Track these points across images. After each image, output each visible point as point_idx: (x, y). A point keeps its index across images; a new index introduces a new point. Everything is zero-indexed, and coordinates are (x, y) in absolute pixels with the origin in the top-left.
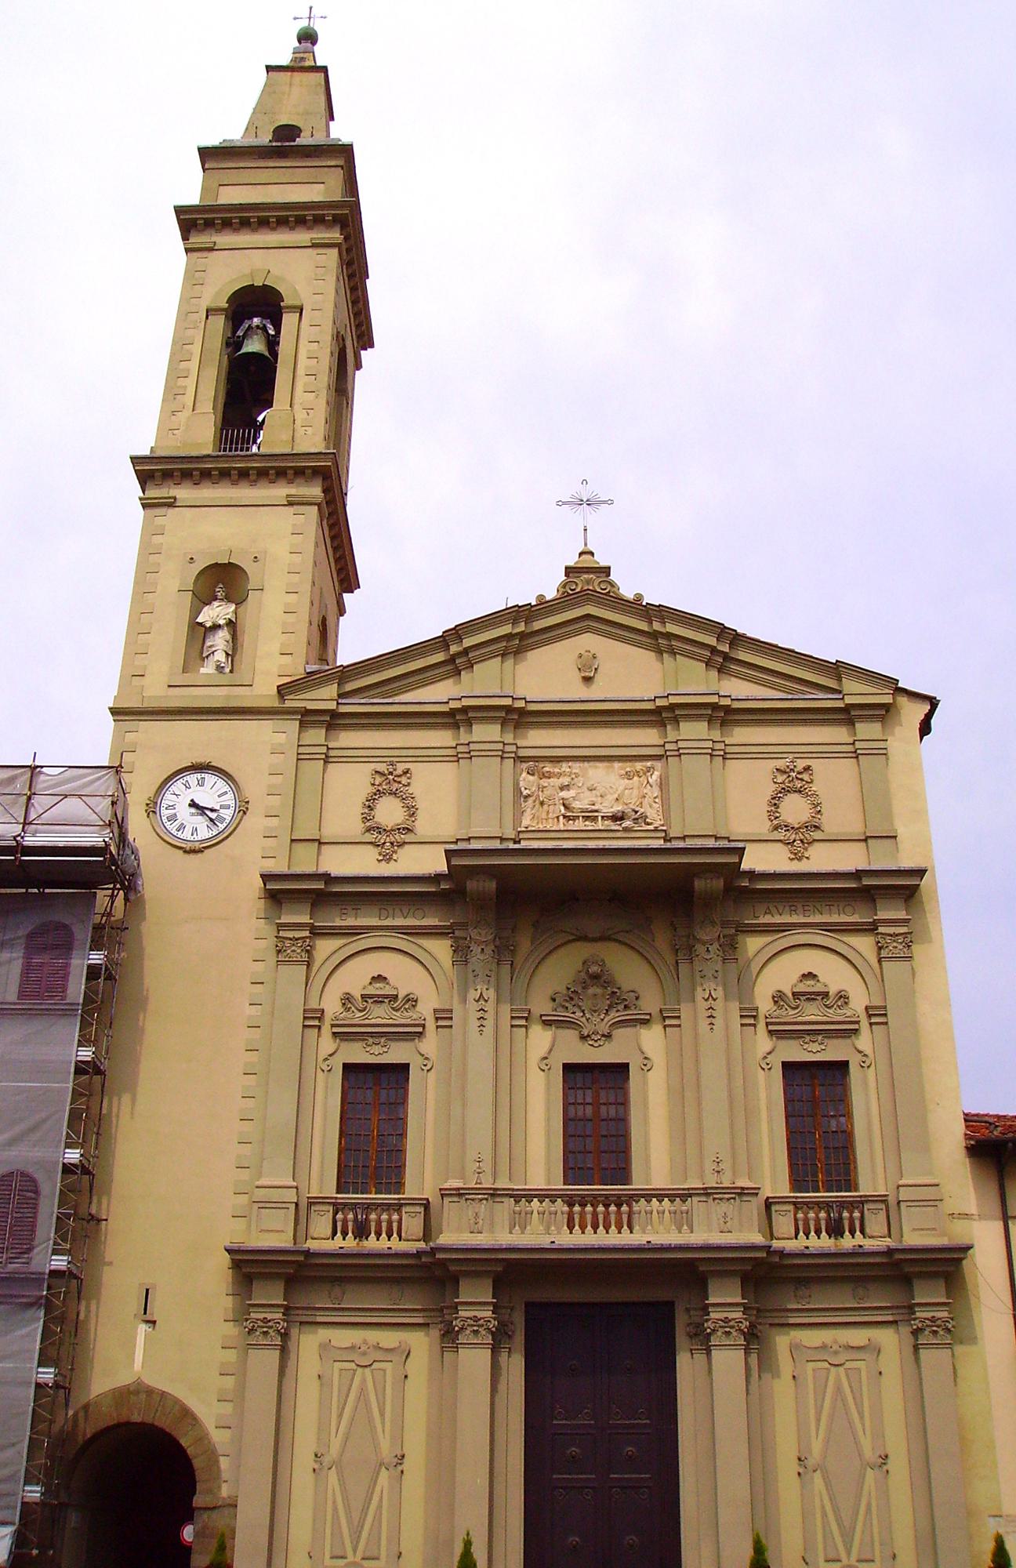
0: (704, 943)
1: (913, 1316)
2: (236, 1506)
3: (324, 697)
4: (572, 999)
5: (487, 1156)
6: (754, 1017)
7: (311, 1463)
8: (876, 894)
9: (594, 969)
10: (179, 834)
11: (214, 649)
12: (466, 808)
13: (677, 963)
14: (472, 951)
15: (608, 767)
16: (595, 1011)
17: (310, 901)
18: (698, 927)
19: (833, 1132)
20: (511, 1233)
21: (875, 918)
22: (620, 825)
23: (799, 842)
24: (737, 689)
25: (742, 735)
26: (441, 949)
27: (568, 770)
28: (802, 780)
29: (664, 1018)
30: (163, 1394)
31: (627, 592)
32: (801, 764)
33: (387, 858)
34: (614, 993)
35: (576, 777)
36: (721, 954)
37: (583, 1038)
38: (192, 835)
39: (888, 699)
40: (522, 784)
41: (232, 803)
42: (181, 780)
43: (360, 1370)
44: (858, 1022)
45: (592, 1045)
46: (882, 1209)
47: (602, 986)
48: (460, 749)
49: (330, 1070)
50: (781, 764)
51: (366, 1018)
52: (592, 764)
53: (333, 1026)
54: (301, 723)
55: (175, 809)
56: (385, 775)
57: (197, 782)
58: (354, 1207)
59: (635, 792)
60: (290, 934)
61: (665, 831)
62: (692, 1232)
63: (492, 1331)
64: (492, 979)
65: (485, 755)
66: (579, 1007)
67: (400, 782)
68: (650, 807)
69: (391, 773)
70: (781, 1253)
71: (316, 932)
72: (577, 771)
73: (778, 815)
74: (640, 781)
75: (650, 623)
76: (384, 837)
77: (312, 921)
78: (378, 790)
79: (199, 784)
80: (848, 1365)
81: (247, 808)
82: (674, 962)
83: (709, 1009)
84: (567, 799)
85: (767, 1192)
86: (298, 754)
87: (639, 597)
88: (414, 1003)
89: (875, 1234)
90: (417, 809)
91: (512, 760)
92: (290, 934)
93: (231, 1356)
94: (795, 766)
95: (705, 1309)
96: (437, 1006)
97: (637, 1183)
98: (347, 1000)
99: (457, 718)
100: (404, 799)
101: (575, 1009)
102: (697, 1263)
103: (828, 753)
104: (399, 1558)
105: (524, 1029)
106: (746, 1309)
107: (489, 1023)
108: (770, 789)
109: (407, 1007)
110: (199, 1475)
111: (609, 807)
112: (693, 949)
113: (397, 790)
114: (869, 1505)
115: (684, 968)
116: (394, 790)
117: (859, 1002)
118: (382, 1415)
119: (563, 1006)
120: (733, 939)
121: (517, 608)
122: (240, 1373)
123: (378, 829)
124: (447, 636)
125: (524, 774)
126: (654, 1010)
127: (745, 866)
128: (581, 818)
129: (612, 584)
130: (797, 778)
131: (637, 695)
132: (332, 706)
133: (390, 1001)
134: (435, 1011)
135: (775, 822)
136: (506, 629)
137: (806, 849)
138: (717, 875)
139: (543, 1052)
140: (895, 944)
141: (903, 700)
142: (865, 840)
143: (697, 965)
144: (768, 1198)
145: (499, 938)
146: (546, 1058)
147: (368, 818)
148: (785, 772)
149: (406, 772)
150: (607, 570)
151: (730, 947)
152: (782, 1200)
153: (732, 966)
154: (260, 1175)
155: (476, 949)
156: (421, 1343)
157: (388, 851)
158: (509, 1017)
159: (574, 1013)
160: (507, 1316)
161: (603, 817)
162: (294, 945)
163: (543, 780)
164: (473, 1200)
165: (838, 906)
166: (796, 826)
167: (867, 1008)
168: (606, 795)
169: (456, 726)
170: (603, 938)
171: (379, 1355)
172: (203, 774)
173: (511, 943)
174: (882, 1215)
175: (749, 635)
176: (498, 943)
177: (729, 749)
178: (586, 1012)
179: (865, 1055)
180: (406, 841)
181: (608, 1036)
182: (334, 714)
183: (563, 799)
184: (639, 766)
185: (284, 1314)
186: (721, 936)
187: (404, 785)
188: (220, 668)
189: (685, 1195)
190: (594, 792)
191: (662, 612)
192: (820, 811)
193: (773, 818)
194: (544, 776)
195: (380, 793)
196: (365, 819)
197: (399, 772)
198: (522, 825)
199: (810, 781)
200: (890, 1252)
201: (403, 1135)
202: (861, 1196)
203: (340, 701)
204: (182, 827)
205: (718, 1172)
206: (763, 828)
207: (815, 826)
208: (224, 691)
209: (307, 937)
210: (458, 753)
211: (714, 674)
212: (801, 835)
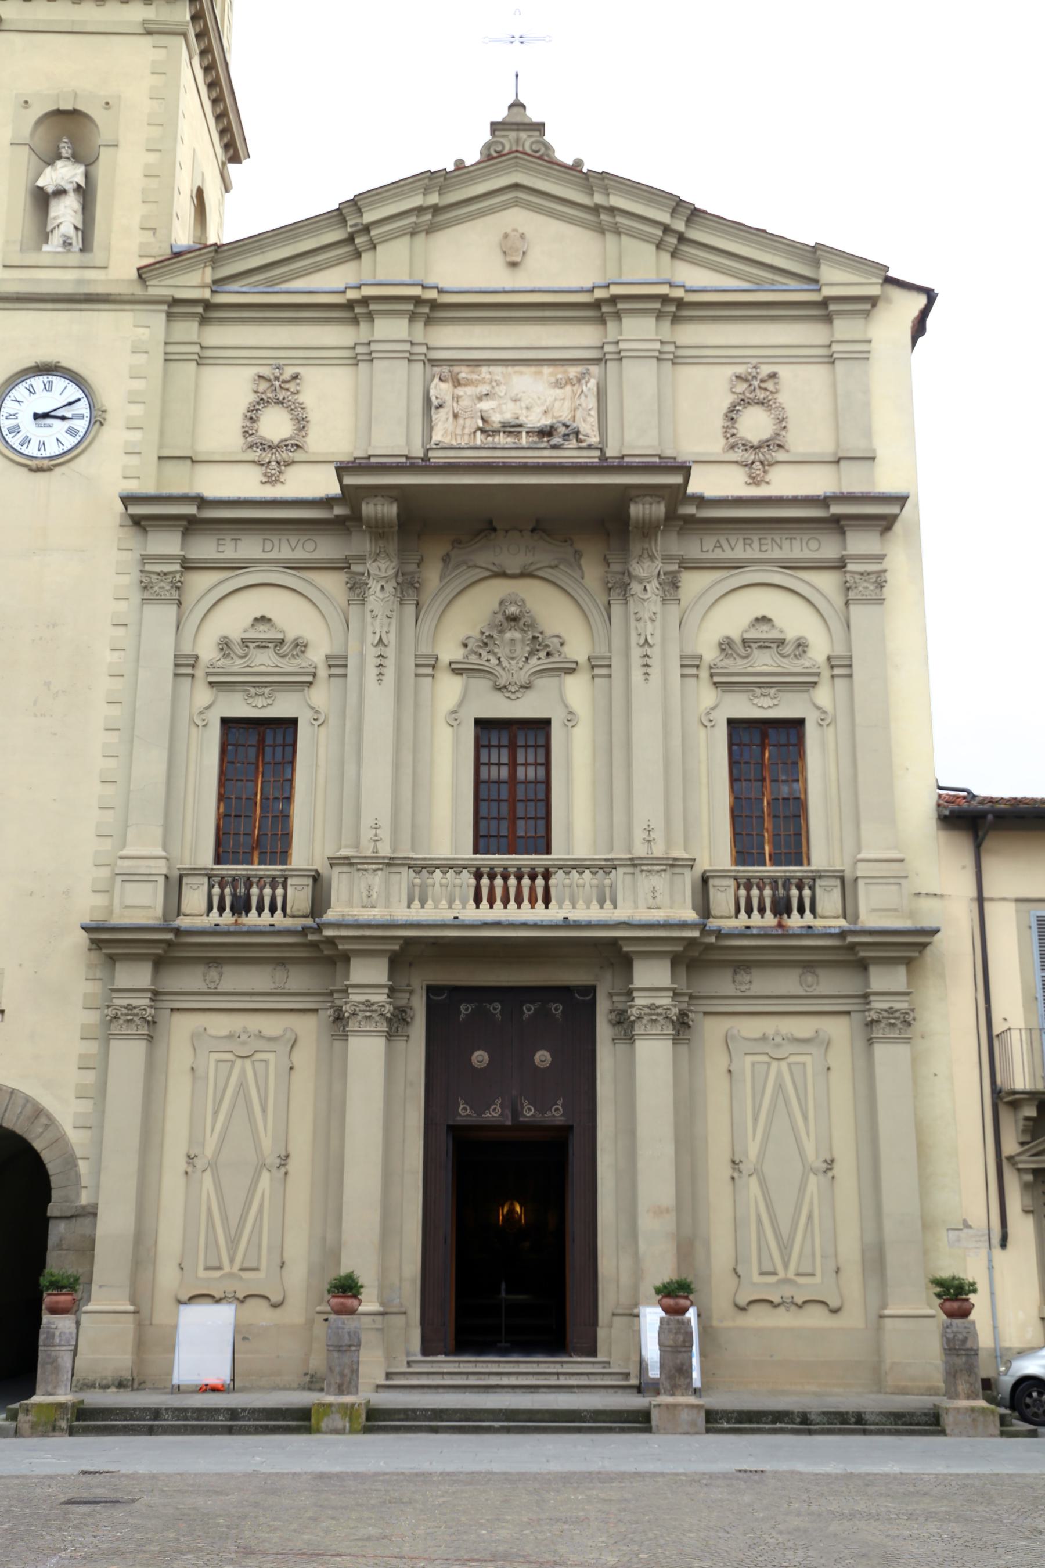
0: (640, 581)
1: (868, 1007)
2: (95, 1215)
4: (486, 644)
5: (386, 823)
6: (698, 667)
7: (182, 1165)
8: (848, 526)
9: (513, 609)
10: (24, 450)
11: (59, 221)
13: (609, 603)
14: (370, 588)
15: (536, 373)
16: (513, 659)
17: (181, 529)
18: (636, 560)
19: (784, 799)
20: (409, 907)
21: (844, 553)
22: (548, 441)
23: (758, 463)
26: (333, 583)
27: (488, 376)
28: (766, 389)
29: (593, 667)
30: (13, 1092)
31: (565, 155)
32: (765, 370)
33: (271, 480)
34: (535, 638)
35: (497, 385)
36: (660, 593)
37: (500, 689)
38: (39, 450)
39: (874, 291)
40: (432, 392)
42: (24, 383)
43: (239, 1062)
44: (818, 675)
45: (509, 698)
46: (836, 886)
47: (523, 630)
48: (360, 349)
49: (205, 726)
50: (741, 370)
51: (248, 666)
52: (517, 368)
53: (208, 674)
54: (170, 316)
55: (17, 418)
56: (270, 380)
58: (235, 880)
59: (567, 404)
60: (158, 568)
61: (601, 450)
62: (615, 908)
63: (387, 1018)
64: (394, 621)
65: (391, 356)
66: (495, 654)
67: (287, 390)
68: (584, 421)
69: (277, 378)
70: (719, 934)
71: (188, 566)
72: (498, 378)
73: (735, 431)
74: (573, 391)
76: (270, 455)
77: (183, 553)
78: (262, 399)
80: (792, 1059)
81: (105, 419)
82: (607, 603)
83: (644, 656)
84: (486, 411)
85: (704, 864)
86: (166, 353)
87: (579, 163)
88: (303, 649)
89: (827, 914)
90: (307, 422)
91: (422, 363)
92: (158, 568)
93: (92, 1048)
94: (758, 373)
95: (629, 994)
96: (328, 652)
97: (558, 852)
98: (225, 645)
100: (292, 410)
101: (491, 657)
102: (620, 942)
104: (282, 1267)
105: (431, 678)
106: (676, 994)
107: (390, 672)
108: (728, 400)
109: (295, 653)
110: (54, 1181)
111: (536, 419)
112: (628, 588)
113: (284, 399)
114: (810, 1217)
115: (617, 609)
116: (281, 398)
117: (819, 651)
118: (264, 1111)
119: (476, 653)
120: (676, 577)
121: (429, 174)
122: (102, 1066)
123: (265, 446)
124: (345, 208)
125: (436, 380)
126: (582, 659)
127: (691, 489)
128: (502, 434)
129: (547, 146)
130: (760, 387)
131: (575, 284)
132: (206, 294)
133: (276, 646)
134: (327, 657)
135: (732, 440)
136: (417, 201)
137: (765, 472)
138: (657, 499)
140: (865, 584)
141: (895, 293)
142: (838, 462)
143: (633, 607)
144: (705, 872)
145: (403, 574)
146: (455, 712)
147: (250, 432)
148: (746, 380)
149: (296, 377)
150: (540, 127)
151: (671, 584)
152: (723, 875)
153: (674, 610)
154: (124, 846)
155: (374, 586)
157: (273, 472)
158: (413, 665)
159: (488, 661)
160: (406, 1001)
161: (527, 433)
162: (162, 581)
163: (459, 388)
164: (366, 870)
165: (801, 539)
166: (756, 443)
167: (829, 658)
168: (531, 407)
169: (355, 321)
170: (523, 575)
171: (260, 1044)
173: (416, 580)
174: (837, 893)
175: (709, 211)
176: (400, 580)
177: (681, 352)
178: (502, 659)
179: (825, 712)
180: (296, 460)
181: (527, 687)
182: (207, 305)
183: (481, 411)
184: (573, 371)
185: (152, 1000)
186: (662, 573)
187: (293, 393)
188: (67, 244)
189: (608, 867)
190: (518, 403)
191: (605, 181)
192: (785, 427)
193: (729, 435)
194: (457, 383)
195: (263, 402)
196: (246, 433)
198: (432, 442)
199: (774, 391)
200: (843, 934)
201: (289, 799)
202: (812, 871)
203: (214, 288)
204: (26, 441)
205: (649, 841)
206: (716, 446)
207: (779, 446)
208: (71, 275)
209: (176, 572)
210: (357, 354)
211: (666, 257)
212: (760, 455)
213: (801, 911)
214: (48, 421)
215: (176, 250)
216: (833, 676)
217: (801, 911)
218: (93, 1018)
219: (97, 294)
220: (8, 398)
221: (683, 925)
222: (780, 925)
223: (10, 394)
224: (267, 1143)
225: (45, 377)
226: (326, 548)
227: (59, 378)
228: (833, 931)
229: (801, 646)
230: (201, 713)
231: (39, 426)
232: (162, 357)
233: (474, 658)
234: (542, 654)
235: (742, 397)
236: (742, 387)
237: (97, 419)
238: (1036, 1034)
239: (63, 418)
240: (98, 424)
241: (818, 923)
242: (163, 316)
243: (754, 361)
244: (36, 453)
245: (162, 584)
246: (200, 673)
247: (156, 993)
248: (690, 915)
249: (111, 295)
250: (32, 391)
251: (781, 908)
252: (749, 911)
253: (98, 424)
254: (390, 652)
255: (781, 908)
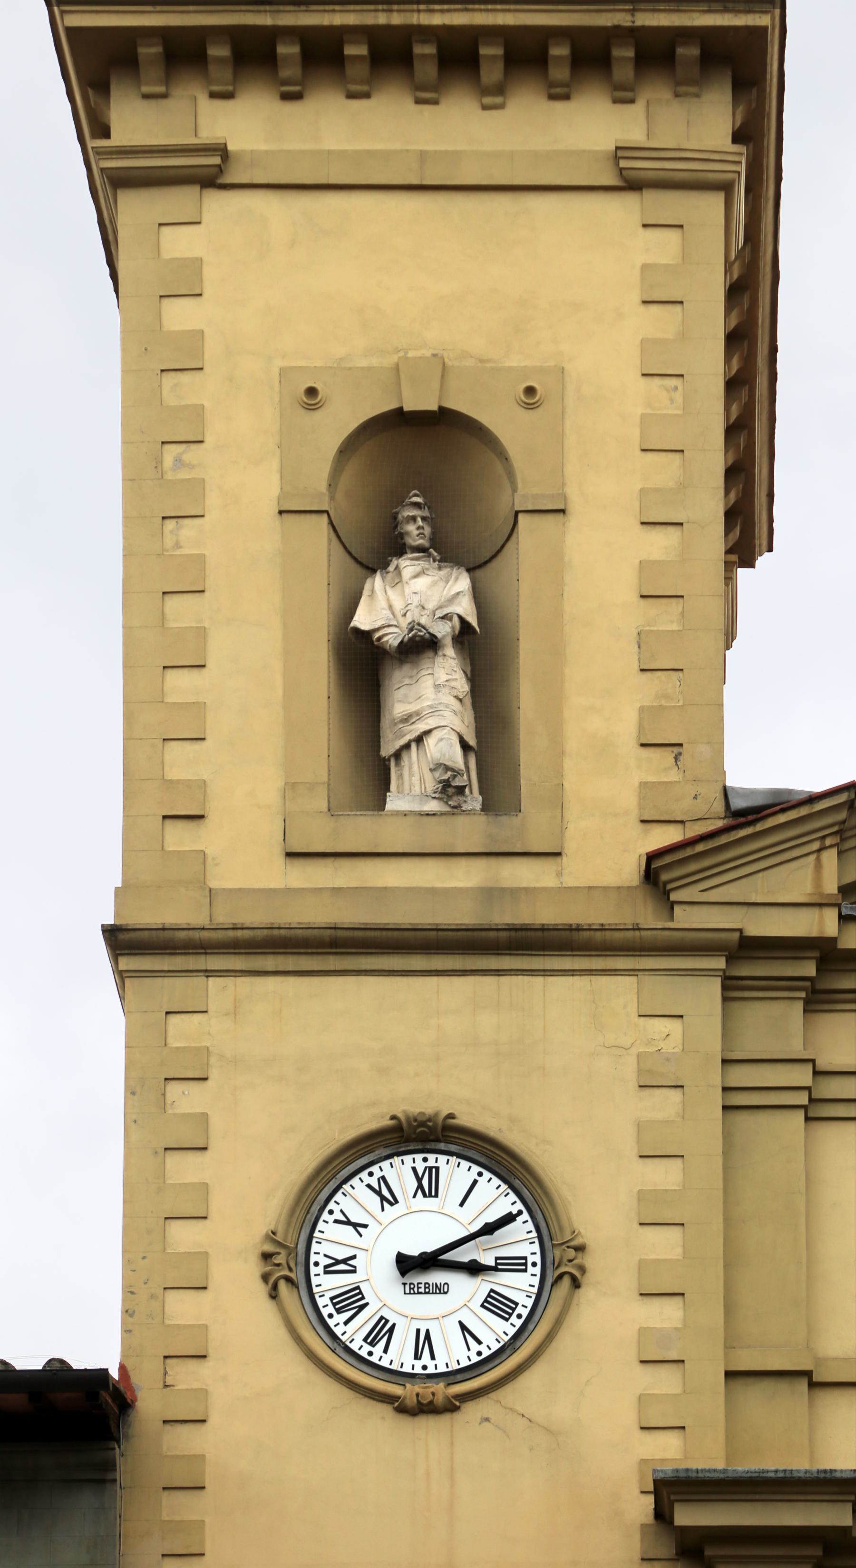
10: (377, 1355)
11: (421, 727)
38: (417, 1356)
42: (364, 1175)
57: (415, 1184)
79: (420, 1186)
81: (582, 1269)
172: (431, 1157)
214: (437, 1277)
215: (738, 803)
219: (543, 929)
220: (325, 1216)
223: (331, 1205)
225: (419, 1157)
227: (454, 1160)
231: (412, 1290)
232: (718, 1099)
239: (474, 1269)
240: (566, 1281)
242: (716, 985)
244: (409, 1364)
249: (579, 929)
250: (388, 1199)
253: (566, 1281)
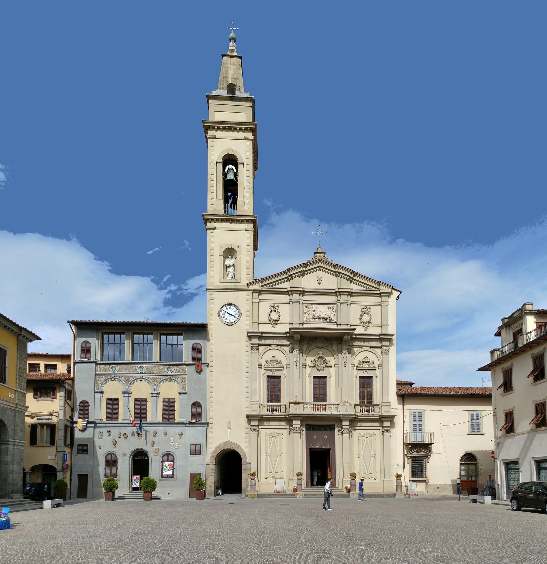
3: (257, 286)
5: (298, 396)
12: (292, 315)
15: (324, 306)
24: (354, 287)
25: (354, 299)
26: (287, 349)
28: (368, 311)
32: (368, 307)
33: (274, 327)
37: (317, 370)
41: (238, 313)
44: (376, 368)
50: (364, 307)
54: (253, 293)
69: (274, 306)
70: (358, 416)
71: (259, 345)
75: (335, 269)
93: (248, 435)
95: (342, 427)
96: (286, 363)
97: (328, 401)
99: (289, 292)
103: (374, 304)
114: (372, 464)
118: (278, 446)
123: (272, 320)
132: (260, 289)
135: (361, 321)
136: (300, 270)
139: (309, 373)
141: (393, 291)
152: (358, 405)
156: (285, 432)
166: (366, 322)
171: (277, 435)
181: (323, 370)
182: (260, 291)
184: (331, 306)
189: (339, 404)
195: (271, 311)
197: (276, 306)
204: (227, 319)
206: (358, 322)
208: (233, 284)
213: (372, 412)
216: (379, 368)
217: (372, 412)
218: (247, 430)
221: (352, 415)
222: (368, 414)
224: (279, 452)
226: (286, 342)
228: (377, 415)
229: (373, 362)
230: (263, 375)
233: (313, 364)
234: (326, 363)
235: (363, 312)
236: (363, 310)
237: (240, 315)
238: (412, 433)
241: (374, 414)
243: (366, 305)
245: (255, 349)
246: (263, 367)
247: (258, 426)
248: (353, 413)
251: (368, 411)
252: (362, 412)
254: (298, 363)
255: (368, 411)
